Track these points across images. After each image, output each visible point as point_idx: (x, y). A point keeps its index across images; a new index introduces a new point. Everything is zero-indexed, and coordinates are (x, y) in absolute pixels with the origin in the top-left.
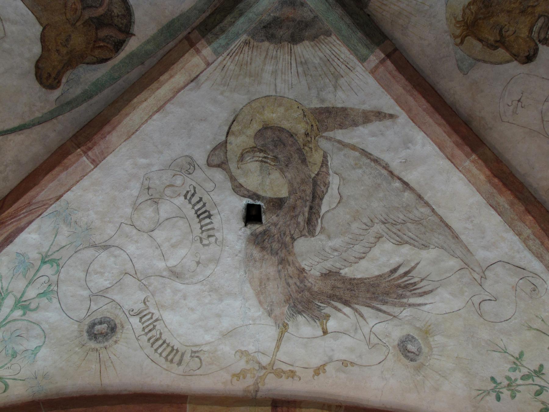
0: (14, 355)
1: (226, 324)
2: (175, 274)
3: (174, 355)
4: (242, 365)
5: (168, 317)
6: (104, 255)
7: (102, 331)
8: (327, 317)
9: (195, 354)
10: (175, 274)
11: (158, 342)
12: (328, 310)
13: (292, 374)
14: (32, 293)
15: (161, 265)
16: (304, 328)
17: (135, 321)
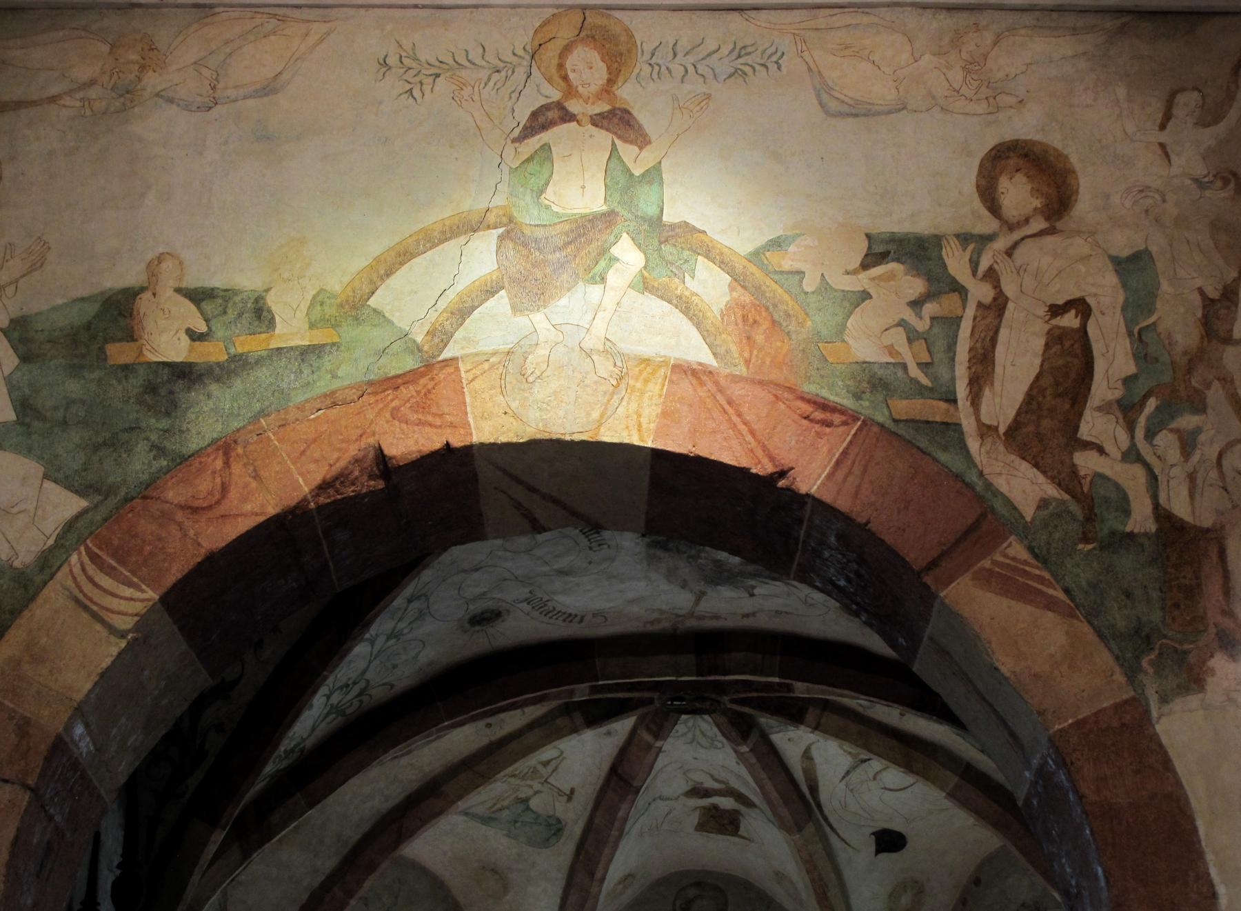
0: (395, 667)
1: (630, 595)
2: (562, 572)
3: (569, 618)
4: (656, 615)
5: (561, 598)
6: (476, 575)
7: (485, 618)
8: (754, 587)
9: (594, 615)
10: (562, 572)
11: (553, 613)
12: (753, 582)
13: (716, 617)
14: (401, 625)
15: (546, 569)
16: (726, 592)
17: (524, 606)
